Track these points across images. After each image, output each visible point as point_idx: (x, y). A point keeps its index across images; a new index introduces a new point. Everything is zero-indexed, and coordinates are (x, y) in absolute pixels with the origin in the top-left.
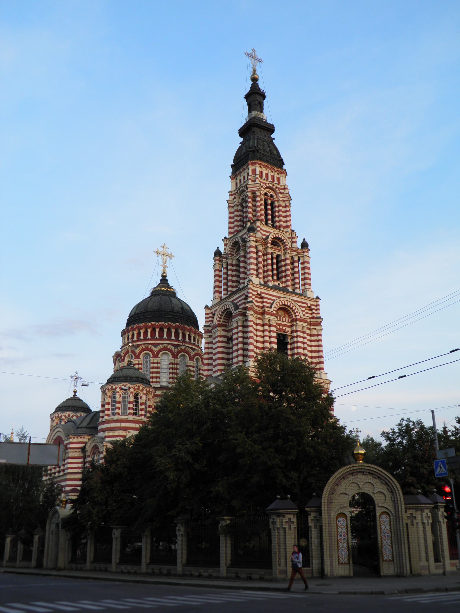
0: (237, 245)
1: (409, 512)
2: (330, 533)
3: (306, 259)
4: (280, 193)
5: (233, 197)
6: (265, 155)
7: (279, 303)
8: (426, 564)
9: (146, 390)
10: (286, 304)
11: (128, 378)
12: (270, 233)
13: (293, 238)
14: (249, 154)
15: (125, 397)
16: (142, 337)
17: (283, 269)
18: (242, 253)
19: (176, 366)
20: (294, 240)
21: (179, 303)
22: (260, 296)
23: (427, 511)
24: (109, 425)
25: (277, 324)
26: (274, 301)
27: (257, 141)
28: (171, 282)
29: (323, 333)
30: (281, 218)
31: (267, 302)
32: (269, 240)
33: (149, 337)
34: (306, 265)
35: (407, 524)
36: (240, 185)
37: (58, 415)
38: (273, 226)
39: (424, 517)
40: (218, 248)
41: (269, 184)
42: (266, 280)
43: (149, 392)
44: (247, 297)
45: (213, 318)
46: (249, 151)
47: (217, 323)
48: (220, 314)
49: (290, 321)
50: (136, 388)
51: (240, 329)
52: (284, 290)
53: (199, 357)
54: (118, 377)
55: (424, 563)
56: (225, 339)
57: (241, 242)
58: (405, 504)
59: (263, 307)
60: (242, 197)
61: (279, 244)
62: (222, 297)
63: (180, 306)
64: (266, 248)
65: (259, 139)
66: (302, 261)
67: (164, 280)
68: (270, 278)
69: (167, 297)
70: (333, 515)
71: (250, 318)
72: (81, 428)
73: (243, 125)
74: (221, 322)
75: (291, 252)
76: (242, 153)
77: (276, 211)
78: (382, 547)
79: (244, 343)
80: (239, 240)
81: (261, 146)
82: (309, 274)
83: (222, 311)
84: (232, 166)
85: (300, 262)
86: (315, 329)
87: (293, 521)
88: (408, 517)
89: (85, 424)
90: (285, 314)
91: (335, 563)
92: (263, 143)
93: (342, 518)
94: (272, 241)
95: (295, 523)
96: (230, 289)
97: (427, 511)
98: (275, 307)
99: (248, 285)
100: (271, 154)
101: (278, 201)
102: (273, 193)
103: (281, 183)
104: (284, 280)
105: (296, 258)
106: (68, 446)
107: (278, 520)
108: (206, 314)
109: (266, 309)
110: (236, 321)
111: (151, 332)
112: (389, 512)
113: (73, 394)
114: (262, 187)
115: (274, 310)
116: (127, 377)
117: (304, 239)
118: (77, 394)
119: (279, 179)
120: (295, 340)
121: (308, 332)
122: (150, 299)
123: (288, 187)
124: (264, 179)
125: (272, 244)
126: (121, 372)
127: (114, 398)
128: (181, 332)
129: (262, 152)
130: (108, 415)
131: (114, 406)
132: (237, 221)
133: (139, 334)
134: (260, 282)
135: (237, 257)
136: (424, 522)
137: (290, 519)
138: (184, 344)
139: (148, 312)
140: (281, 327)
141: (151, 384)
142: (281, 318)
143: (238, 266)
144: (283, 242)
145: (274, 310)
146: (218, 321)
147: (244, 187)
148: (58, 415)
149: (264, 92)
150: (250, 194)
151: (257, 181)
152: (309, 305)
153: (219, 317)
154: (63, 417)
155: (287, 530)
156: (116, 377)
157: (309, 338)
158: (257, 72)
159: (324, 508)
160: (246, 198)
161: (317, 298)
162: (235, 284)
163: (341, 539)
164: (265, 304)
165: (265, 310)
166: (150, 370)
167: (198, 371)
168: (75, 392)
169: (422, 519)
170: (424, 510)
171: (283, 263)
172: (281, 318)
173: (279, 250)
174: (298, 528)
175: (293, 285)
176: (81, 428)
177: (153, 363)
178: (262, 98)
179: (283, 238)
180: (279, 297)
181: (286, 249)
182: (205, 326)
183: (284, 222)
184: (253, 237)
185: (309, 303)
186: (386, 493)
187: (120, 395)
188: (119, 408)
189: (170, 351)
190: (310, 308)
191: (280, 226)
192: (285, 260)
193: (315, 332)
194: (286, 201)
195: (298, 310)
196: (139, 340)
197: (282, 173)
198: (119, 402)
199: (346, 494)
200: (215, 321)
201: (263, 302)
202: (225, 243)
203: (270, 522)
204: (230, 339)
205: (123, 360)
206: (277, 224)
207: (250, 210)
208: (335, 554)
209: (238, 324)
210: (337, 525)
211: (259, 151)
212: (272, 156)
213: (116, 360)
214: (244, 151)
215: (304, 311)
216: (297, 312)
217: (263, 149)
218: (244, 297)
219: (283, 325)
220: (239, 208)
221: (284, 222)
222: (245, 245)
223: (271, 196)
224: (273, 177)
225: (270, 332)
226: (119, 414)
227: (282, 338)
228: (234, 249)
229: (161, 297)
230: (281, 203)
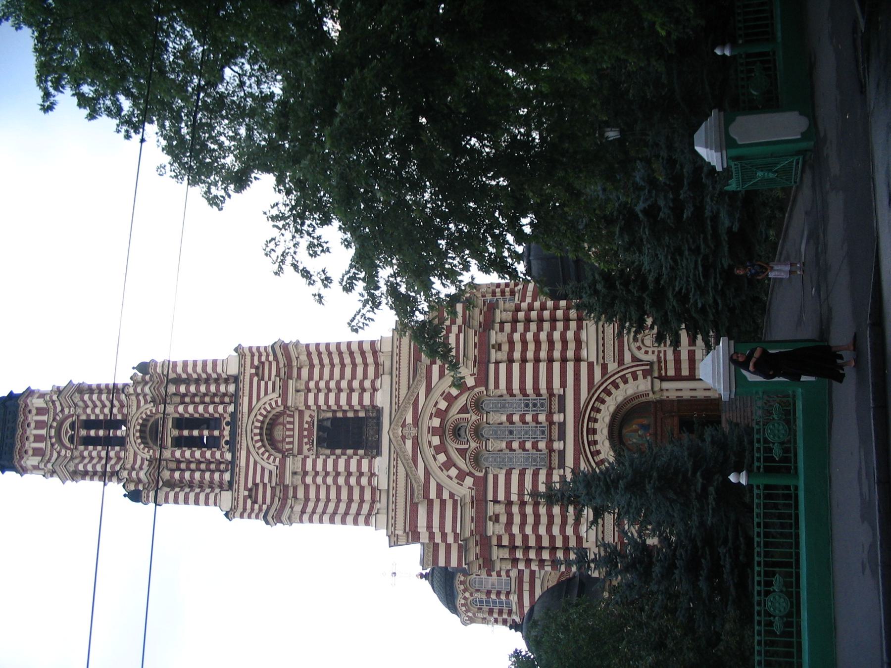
4: (62, 411)
12: (135, 455)
29: (303, 342)
50: (462, 587)
90: (280, 424)
101: (78, 416)
103: (45, 406)
115: (274, 461)
119: (40, 411)
120: (324, 407)
121: (305, 372)
142: (288, 433)
145: (274, 461)
161: (236, 350)
164: (266, 480)
172: (288, 433)
180: (248, 452)
185: (250, 371)
187: (479, 609)
193: (304, 358)
195: (266, 403)
215: (266, 384)
216: (270, 405)
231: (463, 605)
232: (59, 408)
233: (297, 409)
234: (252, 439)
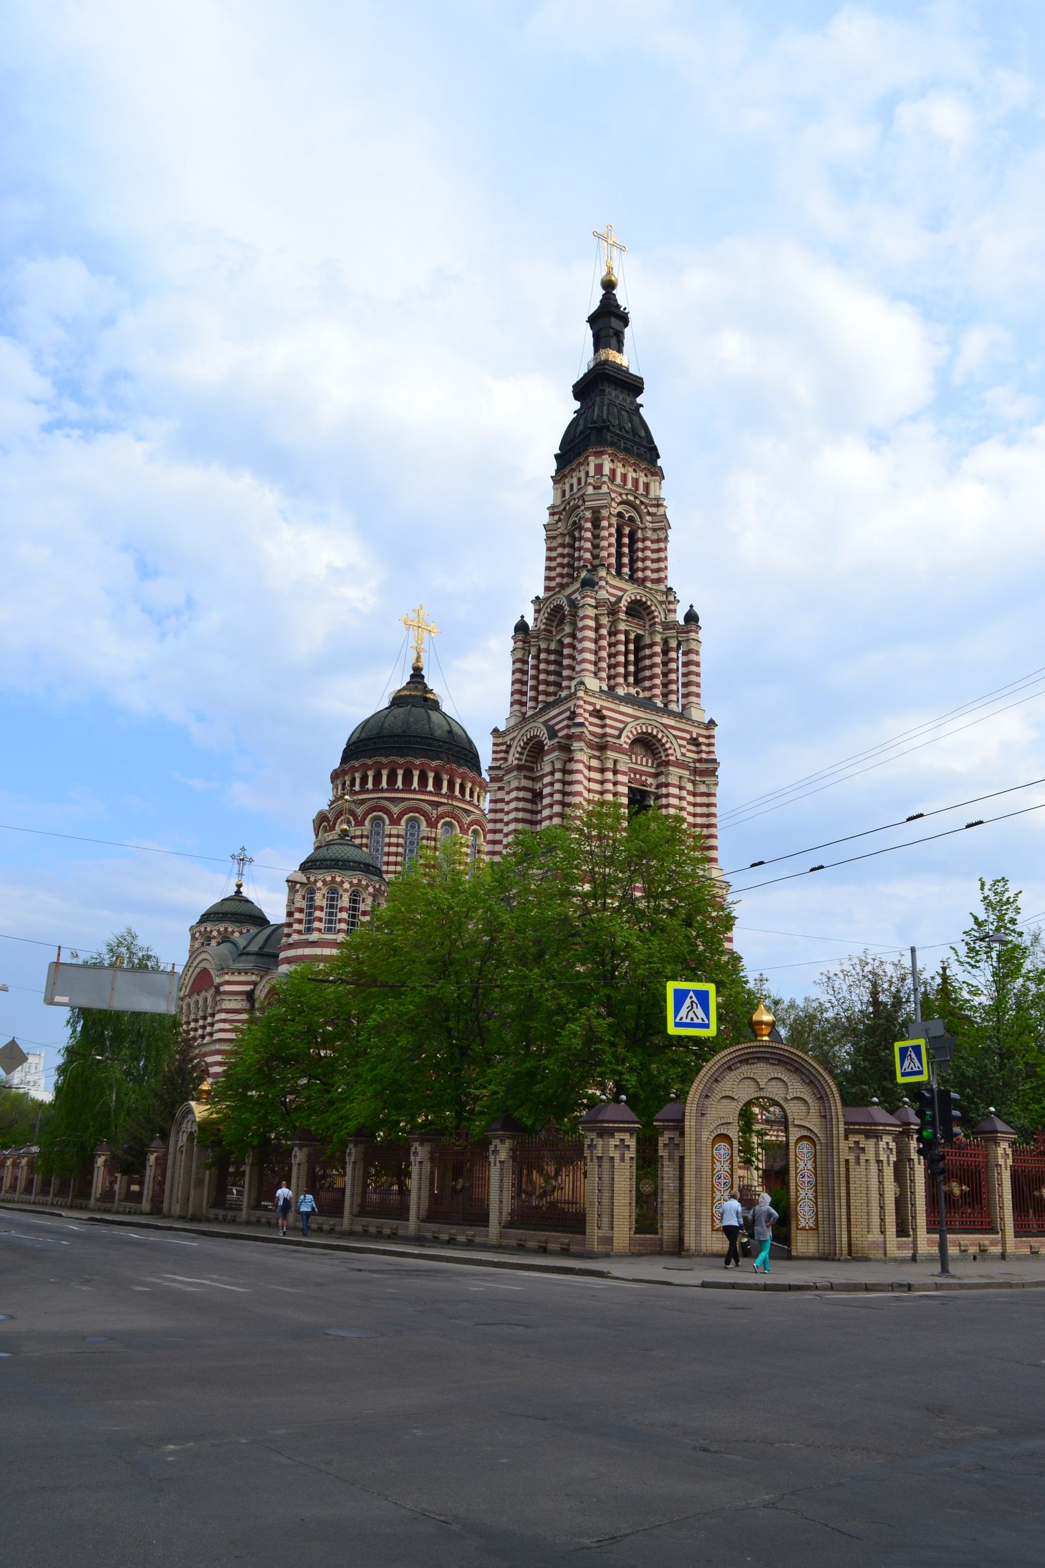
0: (559, 612)
1: (853, 1138)
2: (698, 1170)
3: (693, 645)
4: (649, 513)
5: (556, 517)
6: (623, 437)
7: (636, 729)
8: (881, 1238)
9: (374, 887)
10: (650, 731)
11: (340, 863)
12: (625, 591)
13: (670, 603)
14: (590, 434)
15: (332, 899)
16: (370, 786)
17: (647, 662)
18: (568, 629)
19: (433, 843)
20: (672, 607)
21: (444, 722)
22: (598, 714)
23: (887, 1139)
24: (300, 952)
25: (631, 770)
26: (627, 724)
27: (608, 410)
28: (430, 682)
29: (718, 790)
30: (648, 563)
31: (612, 727)
32: (621, 605)
33: (384, 784)
34: (693, 657)
35: (847, 1161)
36: (571, 496)
37: (206, 928)
38: (632, 579)
39: (881, 1149)
40: (522, 617)
41: (627, 494)
42: (612, 682)
43: (379, 889)
44: (573, 715)
45: (507, 752)
46: (590, 428)
47: (516, 762)
48: (520, 746)
49: (655, 766)
51: (558, 775)
52: (647, 704)
53: (479, 828)
54: (320, 860)
55: (875, 1236)
56: (529, 795)
57: (567, 608)
58: (846, 1124)
59: (604, 735)
60: (573, 519)
61: (641, 613)
62: (526, 713)
63: (447, 727)
64: (614, 623)
65: (612, 404)
66: (686, 649)
67: (417, 675)
68: (621, 680)
69: (422, 710)
70: (706, 1136)
71: (578, 756)
72: (248, 954)
73: (581, 375)
74: (523, 762)
75: (664, 630)
76: (578, 431)
77: (638, 550)
78: (797, 1203)
79: (564, 805)
80: (564, 602)
81: (615, 418)
82: (698, 675)
83: (525, 740)
84: (557, 456)
85: (681, 652)
86: (704, 782)
87: (628, 1146)
88: (850, 1148)
89: (254, 948)
91: (706, 1228)
92: (620, 415)
93: (723, 1144)
94: (627, 608)
95: (633, 1149)
96: (541, 698)
97: (887, 1139)
98: (628, 737)
99: (576, 691)
100: (634, 436)
102: (634, 514)
103: (652, 495)
104: (647, 684)
105: (673, 644)
106: (222, 989)
107: (599, 1142)
108: (495, 744)
109: (609, 739)
110: (550, 761)
111: (388, 776)
112: (814, 1137)
113: (236, 889)
114: (613, 499)
115: (625, 742)
116: (339, 861)
117: (691, 606)
118: (242, 889)
119: (647, 486)
120: (664, 801)
121: (690, 787)
122: (389, 712)
123: (665, 504)
124: (618, 486)
125: (627, 613)
126: (327, 850)
127: (312, 899)
128: (445, 778)
129: (617, 431)
130: (299, 932)
131: (310, 914)
132: (562, 566)
133: (364, 780)
134: (600, 687)
135: (558, 637)
136: (881, 1159)
137: (622, 1140)
138: (450, 802)
139: (384, 736)
140: (638, 776)
141: (384, 876)
142: (639, 758)
143: (559, 653)
144: (649, 610)
145: (625, 742)
146: (519, 759)
147: (579, 498)
148: (206, 928)
149: (626, 311)
150: (588, 514)
151: (605, 489)
152: (695, 736)
153: (518, 752)
154: (215, 933)
155: (617, 1161)
156: (317, 860)
157: (690, 799)
158: (615, 272)
159: (689, 1123)
160: (582, 522)
161: (712, 723)
162: (552, 689)
163: (720, 1183)
165: (608, 741)
166: (382, 849)
167: (477, 855)
168: (239, 886)
169: (877, 1154)
170: (881, 1137)
171: (647, 652)
172: (639, 758)
173: (641, 625)
174: (638, 1158)
175: (665, 695)
176: (248, 954)
177: (390, 836)
178: (621, 324)
179: (649, 603)
180: (637, 718)
181: (655, 623)
182: (491, 768)
183: (653, 571)
184: (591, 597)
186: (810, 1101)
188: (320, 920)
189: (425, 814)
190: (694, 742)
191: (645, 579)
192: (651, 645)
193: (703, 788)
194: (659, 529)
196: (364, 790)
197: (654, 474)
198: (321, 909)
199: (732, 1098)
200: (510, 758)
201: (603, 726)
202: (537, 608)
203: (586, 1146)
204: (537, 796)
205: (333, 828)
206: (640, 574)
207: (588, 545)
208: (706, 1211)
209: (553, 766)
210: (713, 1157)
211: (611, 428)
212: (636, 439)
213: (319, 827)
214: (580, 428)
215: (684, 747)
216: (670, 748)
217: (619, 424)
218: (567, 714)
219: (642, 773)
220: (567, 540)
221: (653, 571)
222: (576, 613)
223: (631, 519)
224: (636, 482)
225: (615, 784)
226: (319, 930)
227: (639, 798)
228: (553, 621)
229: (410, 709)
230: (649, 534)
231: (333, 878)
232: (652, 510)
233: (661, 773)
234: (644, 724)
